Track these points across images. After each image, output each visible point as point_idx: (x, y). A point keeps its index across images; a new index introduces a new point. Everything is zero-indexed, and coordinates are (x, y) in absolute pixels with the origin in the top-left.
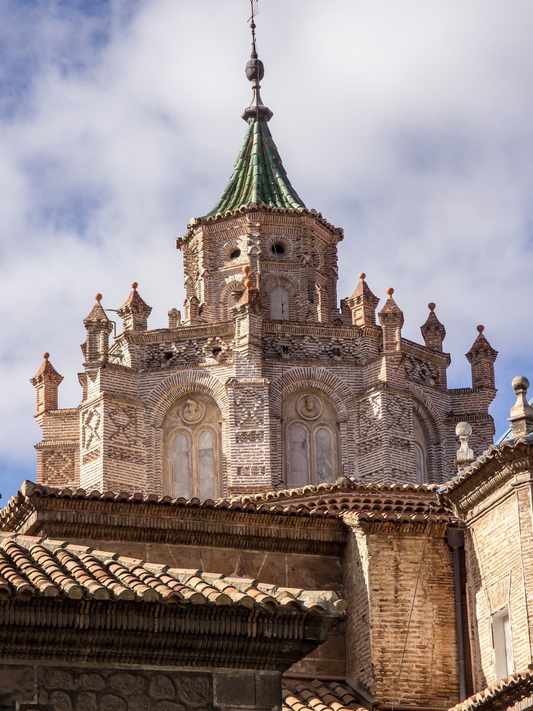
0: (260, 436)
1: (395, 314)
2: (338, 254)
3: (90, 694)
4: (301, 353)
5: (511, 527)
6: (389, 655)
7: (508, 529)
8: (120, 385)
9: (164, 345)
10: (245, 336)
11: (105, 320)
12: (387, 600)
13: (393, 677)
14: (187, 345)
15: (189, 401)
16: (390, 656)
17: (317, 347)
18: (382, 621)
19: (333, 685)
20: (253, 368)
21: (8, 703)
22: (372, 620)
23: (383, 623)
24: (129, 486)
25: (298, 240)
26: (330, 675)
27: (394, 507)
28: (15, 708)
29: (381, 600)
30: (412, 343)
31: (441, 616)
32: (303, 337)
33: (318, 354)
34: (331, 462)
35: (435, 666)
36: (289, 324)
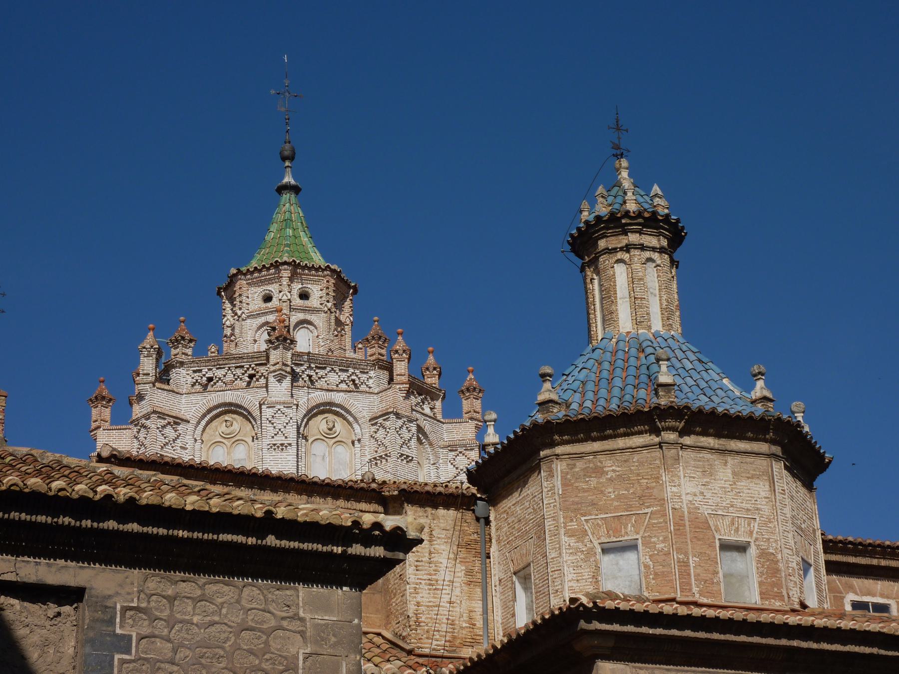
3: (186, 600)
5: (535, 496)
6: (423, 608)
7: (533, 498)
10: (278, 363)
12: (422, 561)
13: (426, 628)
16: (424, 610)
17: (337, 376)
18: (418, 579)
19: (370, 636)
20: (284, 390)
21: (109, 603)
22: (409, 578)
23: (418, 581)
26: (368, 628)
28: (116, 608)
29: (417, 561)
31: (468, 577)
35: (462, 619)
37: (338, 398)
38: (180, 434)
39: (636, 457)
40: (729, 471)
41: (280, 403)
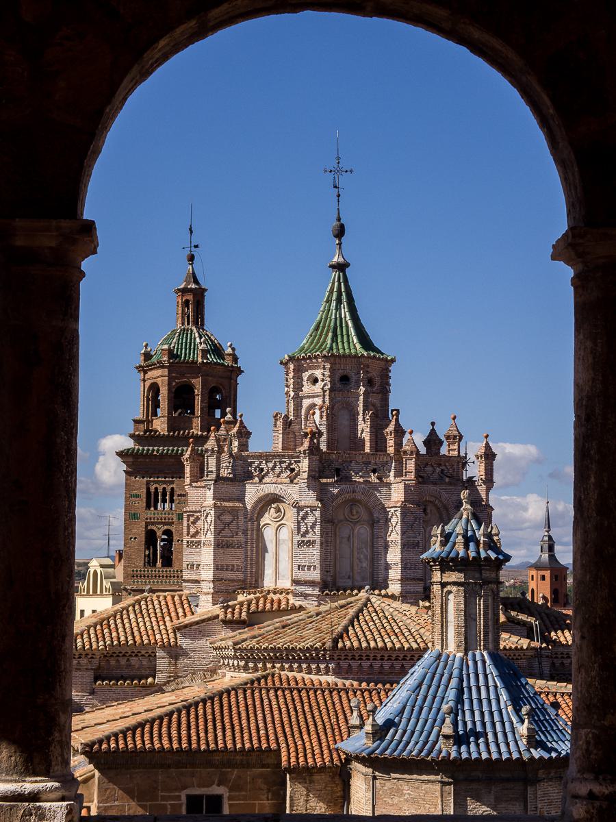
1: (412, 452)
2: (390, 374)
11: (217, 449)
32: (351, 462)
34: (367, 551)
39: (424, 787)
40: (493, 797)
41: (308, 507)
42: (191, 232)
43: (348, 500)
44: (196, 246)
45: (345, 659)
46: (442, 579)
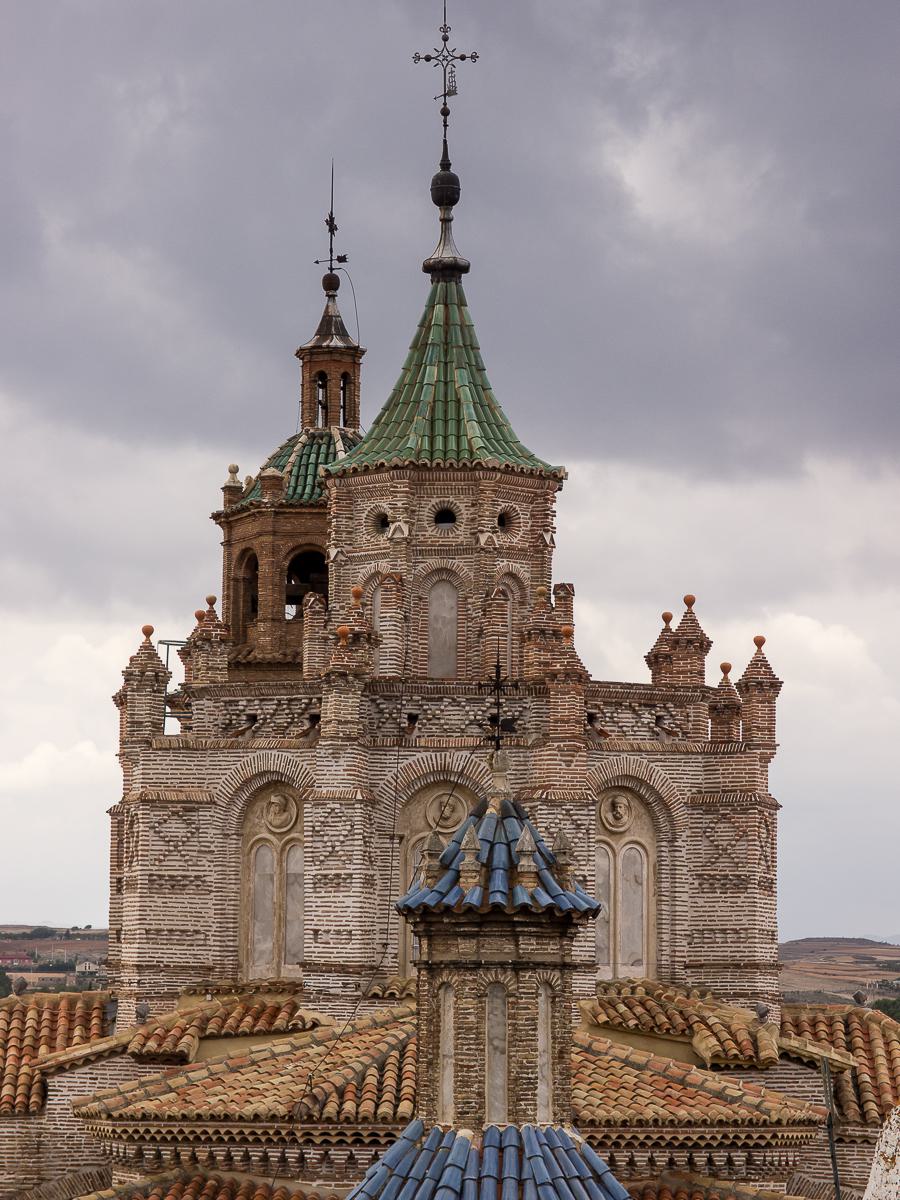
0: (348, 881)
2: (555, 507)
4: (437, 724)
8: (175, 772)
9: (244, 703)
14: (274, 707)
15: (273, 799)
24: (183, 931)
25: (473, 505)
27: (383, 1141)
30: (630, 686)
32: (442, 698)
33: (463, 727)
36: (416, 683)
37: (457, 760)
38: (197, 829)
42: (332, 228)
43: (436, 784)
44: (342, 259)
45: (341, 1142)
46: (430, 954)
